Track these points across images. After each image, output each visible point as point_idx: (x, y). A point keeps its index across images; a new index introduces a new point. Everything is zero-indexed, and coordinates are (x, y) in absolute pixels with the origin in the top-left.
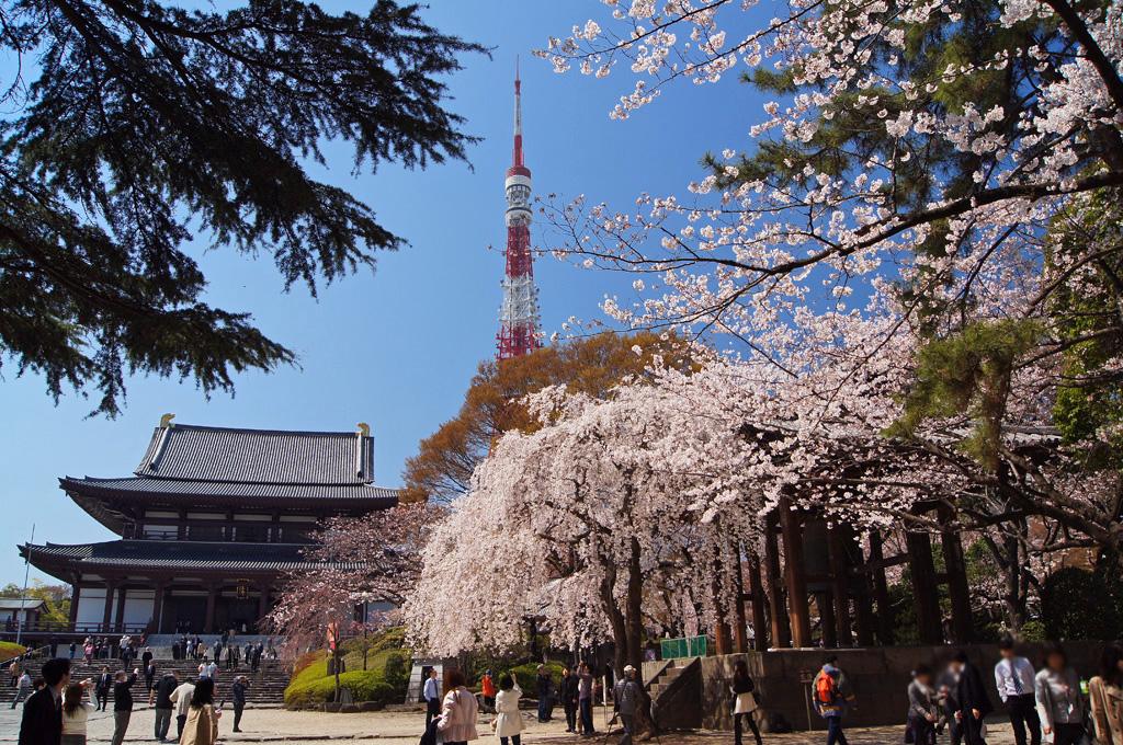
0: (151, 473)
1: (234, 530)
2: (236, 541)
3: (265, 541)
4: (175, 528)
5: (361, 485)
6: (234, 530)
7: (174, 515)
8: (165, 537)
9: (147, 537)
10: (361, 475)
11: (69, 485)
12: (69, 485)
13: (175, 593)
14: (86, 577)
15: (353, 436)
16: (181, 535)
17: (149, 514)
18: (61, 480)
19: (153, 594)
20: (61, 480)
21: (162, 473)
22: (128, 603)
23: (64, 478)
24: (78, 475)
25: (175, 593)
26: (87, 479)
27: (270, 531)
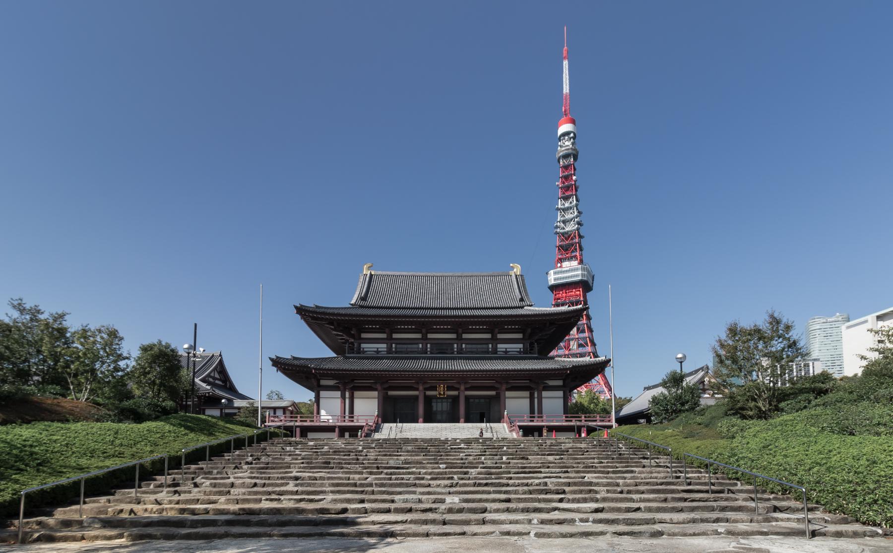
0: (362, 303)
1: (429, 346)
3: (453, 353)
4: (385, 346)
5: (522, 307)
6: (429, 346)
7: (384, 336)
9: (364, 352)
10: (522, 300)
13: (391, 393)
14: (324, 382)
16: (389, 351)
17: (364, 336)
19: (375, 393)
21: (369, 302)
22: (357, 402)
25: (391, 393)
26: (317, 307)
27: (455, 346)
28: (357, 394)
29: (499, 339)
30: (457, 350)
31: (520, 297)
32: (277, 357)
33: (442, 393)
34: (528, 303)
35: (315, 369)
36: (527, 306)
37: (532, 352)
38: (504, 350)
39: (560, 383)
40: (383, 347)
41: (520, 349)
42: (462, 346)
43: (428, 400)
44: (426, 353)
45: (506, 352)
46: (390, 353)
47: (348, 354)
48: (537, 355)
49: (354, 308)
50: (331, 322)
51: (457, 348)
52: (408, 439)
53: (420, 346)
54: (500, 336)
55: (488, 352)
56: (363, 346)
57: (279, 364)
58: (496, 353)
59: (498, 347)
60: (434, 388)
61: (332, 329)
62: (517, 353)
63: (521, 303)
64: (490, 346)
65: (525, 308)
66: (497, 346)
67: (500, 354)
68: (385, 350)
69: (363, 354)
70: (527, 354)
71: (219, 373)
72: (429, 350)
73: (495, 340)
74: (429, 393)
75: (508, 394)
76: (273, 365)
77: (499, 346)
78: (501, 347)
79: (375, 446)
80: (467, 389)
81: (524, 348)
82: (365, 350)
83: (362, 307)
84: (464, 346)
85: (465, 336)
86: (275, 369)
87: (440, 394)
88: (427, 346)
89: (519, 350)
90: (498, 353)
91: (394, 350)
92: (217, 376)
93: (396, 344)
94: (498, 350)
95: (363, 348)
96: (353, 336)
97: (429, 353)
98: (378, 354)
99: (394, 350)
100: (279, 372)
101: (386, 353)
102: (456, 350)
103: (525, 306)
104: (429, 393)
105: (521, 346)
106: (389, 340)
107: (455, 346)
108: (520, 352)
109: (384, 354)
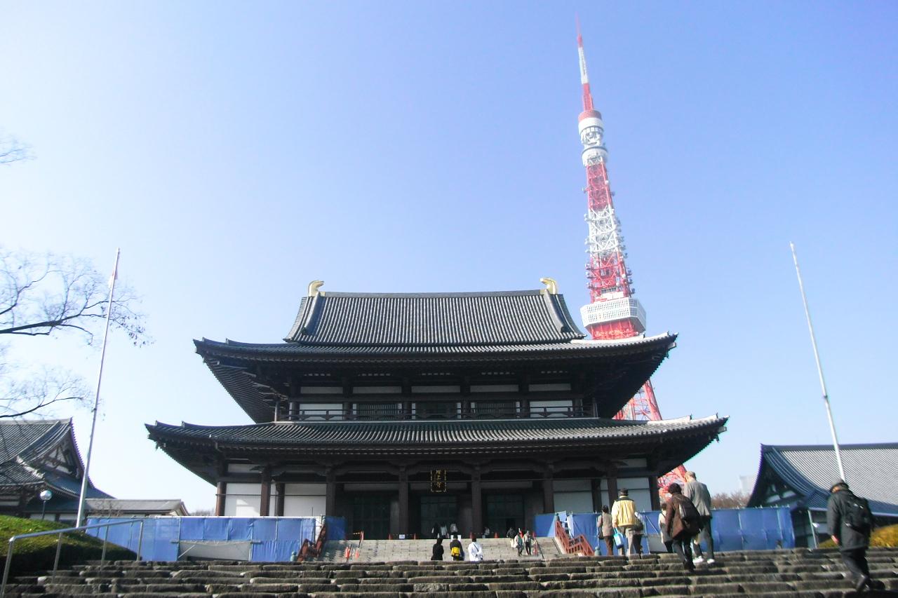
1: (414, 406)
2: (419, 418)
3: (455, 417)
4: (340, 406)
5: (568, 341)
6: (414, 406)
7: (338, 390)
8: (327, 417)
11: (206, 349)
12: (206, 349)
13: (351, 486)
14: (235, 468)
15: (537, 293)
16: (348, 415)
17: (305, 390)
18: (196, 342)
20: (196, 342)
23: (201, 340)
24: (219, 337)
25: (351, 486)
27: (459, 405)
28: (290, 487)
29: (533, 392)
30: (462, 412)
31: (562, 325)
32: (159, 424)
33: (439, 484)
34: (576, 334)
35: (220, 442)
36: (576, 338)
37: (587, 412)
38: (542, 410)
39: (640, 463)
40: (336, 409)
41: (569, 408)
42: (470, 405)
43: (415, 500)
44: (410, 418)
45: (545, 414)
46: (348, 419)
47: (277, 421)
48: (597, 418)
49: (291, 345)
50: (252, 367)
51: (462, 409)
52: (416, 563)
53: (400, 406)
54: (533, 388)
55: (514, 415)
56: (303, 407)
57: (165, 437)
58: (528, 416)
59: (531, 406)
60: (424, 477)
61: (252, 379)
62: (562, 415)
63: (564, 334)
64: (518, 404)
65: (572, 341)
66: (529, 405)
67: (535, 418)
68: (340, 413)
69: (303, 420)
70: (580, 416)
71: (66, 453)
72: (414, 412)
73: (527, 397)
74: (418, 486)
75: (558, 484)
76: (150, 437)
77: (533, 404)
78: (537, 406)
79: (338, 582)
80: (485, 477)
81: (573, 407)
82: (306, 413)
83: (303, 344)
84: (473, 405)
85: (475, 389)
86: (154, 444)
87: (435, 487)
88: (411, 406)
89: (566, 410)
90: (532, 416)
91: (355, 413)
92: (61, 458)
93: (359, 404)
94: (532, 410)
95: (304, 411)
96: (286, 391)
97: (414, 417)
98: (327, 420)
99: (355, 413)
100: (160, 449)
101: (341, 418)
102: (460, 411)
103: (572, 339)
104: (418, 486)
105: (569, 403)
106: (346, 398)
107: (459, 405)
108: (568, 414)
109: (339, 420)
